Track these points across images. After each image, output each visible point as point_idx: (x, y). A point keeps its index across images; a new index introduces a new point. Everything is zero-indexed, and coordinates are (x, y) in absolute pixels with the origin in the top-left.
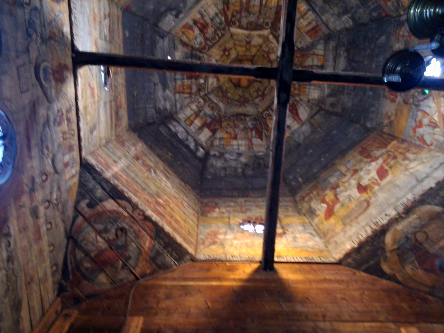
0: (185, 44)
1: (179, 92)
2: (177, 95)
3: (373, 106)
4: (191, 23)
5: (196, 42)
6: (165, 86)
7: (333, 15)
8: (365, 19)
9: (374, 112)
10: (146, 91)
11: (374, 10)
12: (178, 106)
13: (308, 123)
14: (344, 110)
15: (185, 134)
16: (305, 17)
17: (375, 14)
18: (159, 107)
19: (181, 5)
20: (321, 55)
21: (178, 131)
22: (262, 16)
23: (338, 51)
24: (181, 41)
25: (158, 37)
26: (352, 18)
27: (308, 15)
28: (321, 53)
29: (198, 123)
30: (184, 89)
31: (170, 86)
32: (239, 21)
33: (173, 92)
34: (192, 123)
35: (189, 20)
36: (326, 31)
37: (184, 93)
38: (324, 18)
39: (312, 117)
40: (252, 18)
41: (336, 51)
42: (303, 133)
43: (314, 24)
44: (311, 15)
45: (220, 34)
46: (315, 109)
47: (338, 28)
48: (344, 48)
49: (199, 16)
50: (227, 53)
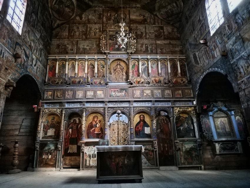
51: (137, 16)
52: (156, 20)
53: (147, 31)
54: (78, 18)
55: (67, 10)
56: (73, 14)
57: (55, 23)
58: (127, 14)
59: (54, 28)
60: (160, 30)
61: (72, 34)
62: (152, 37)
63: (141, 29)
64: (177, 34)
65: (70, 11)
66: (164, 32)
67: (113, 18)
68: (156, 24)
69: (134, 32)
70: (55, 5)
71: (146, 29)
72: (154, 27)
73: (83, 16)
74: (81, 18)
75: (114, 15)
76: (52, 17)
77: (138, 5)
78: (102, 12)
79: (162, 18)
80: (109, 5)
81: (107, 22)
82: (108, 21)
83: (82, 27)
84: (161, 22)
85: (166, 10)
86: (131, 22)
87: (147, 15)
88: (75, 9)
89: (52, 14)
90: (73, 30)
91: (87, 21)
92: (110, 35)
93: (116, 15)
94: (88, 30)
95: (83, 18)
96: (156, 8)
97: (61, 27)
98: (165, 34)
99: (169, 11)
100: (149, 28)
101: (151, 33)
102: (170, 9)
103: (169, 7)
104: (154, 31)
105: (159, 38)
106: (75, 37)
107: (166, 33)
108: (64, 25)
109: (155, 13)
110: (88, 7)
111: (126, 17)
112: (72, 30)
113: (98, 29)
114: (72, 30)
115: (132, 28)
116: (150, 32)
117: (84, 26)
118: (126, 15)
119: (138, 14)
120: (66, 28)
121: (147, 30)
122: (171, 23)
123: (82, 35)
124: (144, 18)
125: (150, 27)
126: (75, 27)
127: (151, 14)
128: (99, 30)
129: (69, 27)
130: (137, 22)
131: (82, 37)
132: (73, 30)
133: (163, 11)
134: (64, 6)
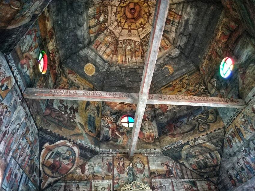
0: (168, 39)
1: (178, 14)
16: (103, 52)
20: (91, 34)
22: (124, 49)
24: (169, 41)
25: (182, 47)
27: (102, 53)
30: (174, 15)
32: (136, 46)
33: (182, 17)
38: (94, 53)
40: (129, 48)
43: (98, 49)
44: (101, 53)
45: (146, 39)
50: (142, 25)
51: (158, 165)
54: (79, 171)
55: (66, 162)
56: (73, 166)
57: (45, 182)
58: (144, 162)
59: (42, 189)
60: (192, 187)
63: (167, 187)
65: (69, 163)
67: (127, 170)
68: (186, 177)
70: (48, 160)
71: (173, 186)
73: (87, 167)
74: (83, 171)
75: (128, 165)
76: (42, 176)
77: (158, 150)
78: (112, 161)
79: (192, 169)
80: (121, 150)
81: (119, 177)
82: (121, 175)
83: (83, 185)
84: (192, 175)
85: (197, 160)
86: (152, 176)
87: (171, 163)
88: (77, 159)
91: (91, 176)
93: (131, 164)
95: (87, 171)
96: (183, 156)
97: (54, 186)
99: (202, 162)
102: (203, 160)
103: (201, 157)
108: (58, 184)
109: (181, 162)
110: (94, 153)
111: (144, 168)
115: (154, 186)
117: (86, 185)
118: (144, 164)
119: (159, 163)
120: (60, 188)
121: (175, 188)
122: (205, 176)
124: (167, 168)
125: (178, 183)
126: (73, 186)
129: (65, 186)
133: (193, 161)
134: (61, 158)
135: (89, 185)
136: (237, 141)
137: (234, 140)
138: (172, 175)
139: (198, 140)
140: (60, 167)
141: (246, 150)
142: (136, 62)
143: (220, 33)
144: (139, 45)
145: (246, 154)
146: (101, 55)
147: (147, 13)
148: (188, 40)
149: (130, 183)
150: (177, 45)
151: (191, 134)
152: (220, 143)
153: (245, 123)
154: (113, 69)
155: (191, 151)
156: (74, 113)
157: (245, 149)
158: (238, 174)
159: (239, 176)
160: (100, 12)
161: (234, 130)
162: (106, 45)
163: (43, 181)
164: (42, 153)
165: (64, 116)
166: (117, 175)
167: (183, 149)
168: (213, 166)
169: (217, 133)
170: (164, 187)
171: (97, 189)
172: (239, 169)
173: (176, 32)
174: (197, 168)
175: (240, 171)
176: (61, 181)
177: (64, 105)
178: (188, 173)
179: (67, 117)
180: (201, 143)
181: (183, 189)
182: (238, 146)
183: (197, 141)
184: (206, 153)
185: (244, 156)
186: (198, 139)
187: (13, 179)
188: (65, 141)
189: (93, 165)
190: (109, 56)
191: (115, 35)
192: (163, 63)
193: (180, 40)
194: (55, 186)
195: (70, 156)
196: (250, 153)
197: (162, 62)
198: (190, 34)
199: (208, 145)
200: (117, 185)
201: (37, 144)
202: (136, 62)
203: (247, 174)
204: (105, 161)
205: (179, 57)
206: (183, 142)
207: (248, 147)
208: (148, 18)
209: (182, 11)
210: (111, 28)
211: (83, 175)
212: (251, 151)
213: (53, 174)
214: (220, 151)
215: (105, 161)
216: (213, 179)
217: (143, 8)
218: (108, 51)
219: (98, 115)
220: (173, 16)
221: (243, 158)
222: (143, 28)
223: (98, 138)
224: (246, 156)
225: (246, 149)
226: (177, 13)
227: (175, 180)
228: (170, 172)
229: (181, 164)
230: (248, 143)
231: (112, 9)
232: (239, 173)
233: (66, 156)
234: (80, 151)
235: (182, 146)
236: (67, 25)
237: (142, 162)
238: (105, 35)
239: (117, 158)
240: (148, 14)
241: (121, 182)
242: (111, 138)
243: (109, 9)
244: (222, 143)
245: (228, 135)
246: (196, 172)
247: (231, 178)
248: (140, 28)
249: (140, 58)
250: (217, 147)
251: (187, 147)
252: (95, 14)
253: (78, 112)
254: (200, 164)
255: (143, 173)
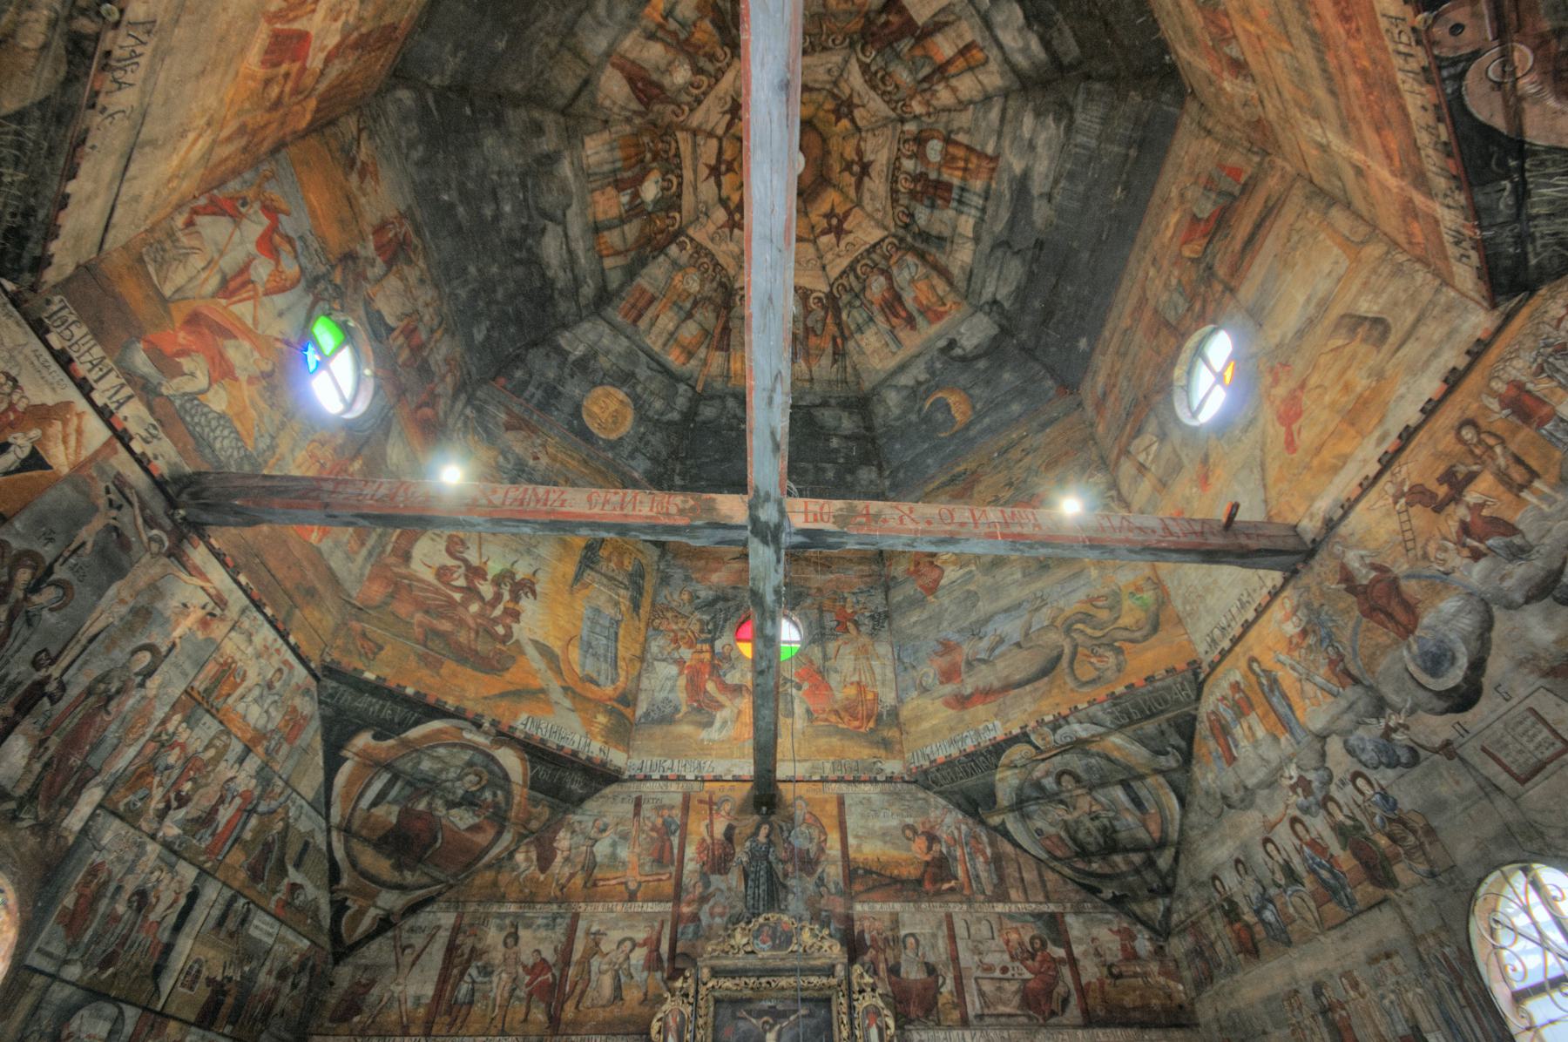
0: (944, 273)
1: (982, 155)
2: (990, 150)
3: (422, 163)
4: (920, 320)
5: (913, 269)
6: (1021, 186)
7: (607, 352)
8: (536, 357)
9: (412, 145)
10: (1081, 188)
11: (525, 384)
12: (994, 114)
13: (594, 61)
14: (499, 121)
15: (998, 18)
16: (665, 335)
17: (519, 374)
18: (1058, 127)
19: (938, 365)
21: (1020, 30)
23: (570, 275)
24: (950, 283)
25: (1006, 305)
26: (562, 353)
27: (660, 342)
28: (608, 263)
29: (944, 47)
30: (967, 161)
31: (1006, 185)
33: (1002, 163)
34: (964, 51)
35: (928, 331)
36: (609, 311)
37: (969, 148)
38: (625, 342)
39: (586, 82)
41: (575, 279)
42: (600, 24)
43: (643, 324)
45: (852, 277)
46: (582, 105)
47: (586, 325)
48: (559, 285)
49: (903, 334)
50: (834, 221)
52: (1011, 870)
53: (966, 958)
55: (462, 819)
56: (499, 834)
57: (361, 912)
58: (824, 821)
60: (1044, 945)
61: (464, 988)
62: (1001, 1009)
63: (922, 941)
64: (1162, 980)
65: (477, 820)
66: (1072, 961)
67: (741, 855)
68: (1013, 894)
69: (882, 966)
71: (952, 937)
72: (1008, 923)
73: (563, 841)
74: (545, 862)
75: (749, 831)
78: (677, 813)
79: (1044, 856)
81: (707, 884)
82: (715, 879)
85: (1067, 817)
86: (857, 887)
87: (950, 822)
89: (343, 863)
90: (475, 953)
91: (579, 880)
92: (717, 1001)
93: (764, 830)
94: (576, 956)
96: (1004, 796)
98: (1084, 981)
100: (972, 931)
101: (990, 969)
104: (1006, 957)
105: (1053, 1014)
106: (477, 1009)
107: (1091, 972)
108: (424, 918)
109: (995, 820)
112: (469, 961)
113: (644, 944)
114: (467, 951)
116: (989, 959)
120: (432, 937)
121: (961, 945)
122: (1108, 894)
123: (530, 995)
124: (930, 849)
125: (979, 920)
127: (970, 821)
128: (648, 959)
129: (456, 930)
130: (895, 880)
131: (525, 1020)
132: (475, 953)
133: (1048, 819)
134: (439, 802)
135: (562, 925)
136: (1260, 733)
137: (1245, 726)
138: (953, 883)
139: (1068, 723)
140: (435, 839)
141: (1310, 782)
142: (811, 380)
143: (1174, 219)
144: (824, 307)
145: (1306, 804)
146: (657, 348)
147: (853, 162)
148: (1032, 272)
149: (749, 922)
150: (983, 300)
151: (1038, 694)
152: (1175, 739)
153: (1298, 646)
154: (708, 412)
155: (1037, 774)
156: (516, 598)
157: (1301, 778)
158: (1266, 900)
159: (1271, 906)
160: (642, 161)
161: (1245, 677)
162: (681, 308)
163: (348, 908)
164: (340, 779)
165: (461, 609)
166: (696, 877)
167: (1004, 760)
168: (1139, 847)
169: (1157, 690)
170: (911, 940)
171: (597, 944)
172: (1273, 873)
173: (977, 239)
174: (1068, 854)
175: (1279, 886)
176: (443, 905)
177: (465, 561)
178: (1025, 875)
179: (475, 616)
180: (1084, 735)
181: (998, 955)
182: (1268, 762)
183: (1065, 729)
184: (1104, 784)
185: (1297, 813)
186: (1071, 719)
187: (114, 918)
188: (455, 722)
189: (593, 833)
190: (690, 355)
191: (717, 264)
192: (927, 381)
193: (995, 275)
194: (412, 930)
195: (483, 788)
196: (1332, 799)
197: (922, 377)
198: (1040, 244)
199: (1119, 748)
200: (691, 928)
201: (312, 735)
202: (811, 380)
203: (1312, 905)
204: (648, 814)
205: (993, 350)
206: (999, 734)
207: (1316, 769)
208: (859, 185)
209: (1000, 134)
210: (699, 234)
211: (542, 877)
212: (1333, 787)
213: (401, 872)
214: (1175, 776)
215: (647, 810)
216: (1148, 908)
217: (834, 143)
218: (690, 331)
219: (636, 606)
220: (961, 164)
221: (1294, 821)
222: (839, 231)
223: (627, 712)
224: (1306, 810)
225: (1311, 776)
226: (978, 148)
227: (965, 907)
228: (940, 868)
229: (995, 829)
230: (1318, 746)
231: (695, 145)
232: (1273, 891)
233: (460, 792)
234: (533, 768)
235: (998, 748)
236: (488, 212)
237: (817, 819)
238: (675, 264)
239: (701, 802)
240: (856, 168)
241: (712, 915)
242: (684, 709)
243: (685, 149)
244: (1183, 737)
245: (1210, 703)
246: (1067, 871)
247: (1231, 912)
248: (824, 233)
249: (826, 361)
250: (1162, 759)
251: (1018, 752)
252: (619, 165)
253: (534, 593)
254: (1081, 835)
255: (814, 871)
